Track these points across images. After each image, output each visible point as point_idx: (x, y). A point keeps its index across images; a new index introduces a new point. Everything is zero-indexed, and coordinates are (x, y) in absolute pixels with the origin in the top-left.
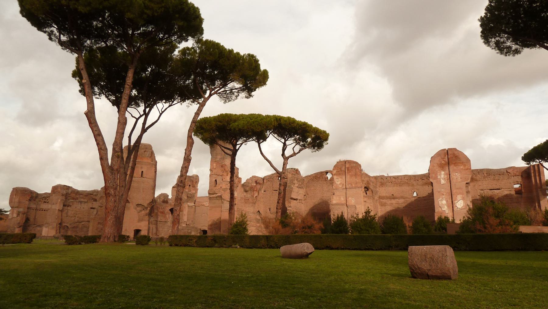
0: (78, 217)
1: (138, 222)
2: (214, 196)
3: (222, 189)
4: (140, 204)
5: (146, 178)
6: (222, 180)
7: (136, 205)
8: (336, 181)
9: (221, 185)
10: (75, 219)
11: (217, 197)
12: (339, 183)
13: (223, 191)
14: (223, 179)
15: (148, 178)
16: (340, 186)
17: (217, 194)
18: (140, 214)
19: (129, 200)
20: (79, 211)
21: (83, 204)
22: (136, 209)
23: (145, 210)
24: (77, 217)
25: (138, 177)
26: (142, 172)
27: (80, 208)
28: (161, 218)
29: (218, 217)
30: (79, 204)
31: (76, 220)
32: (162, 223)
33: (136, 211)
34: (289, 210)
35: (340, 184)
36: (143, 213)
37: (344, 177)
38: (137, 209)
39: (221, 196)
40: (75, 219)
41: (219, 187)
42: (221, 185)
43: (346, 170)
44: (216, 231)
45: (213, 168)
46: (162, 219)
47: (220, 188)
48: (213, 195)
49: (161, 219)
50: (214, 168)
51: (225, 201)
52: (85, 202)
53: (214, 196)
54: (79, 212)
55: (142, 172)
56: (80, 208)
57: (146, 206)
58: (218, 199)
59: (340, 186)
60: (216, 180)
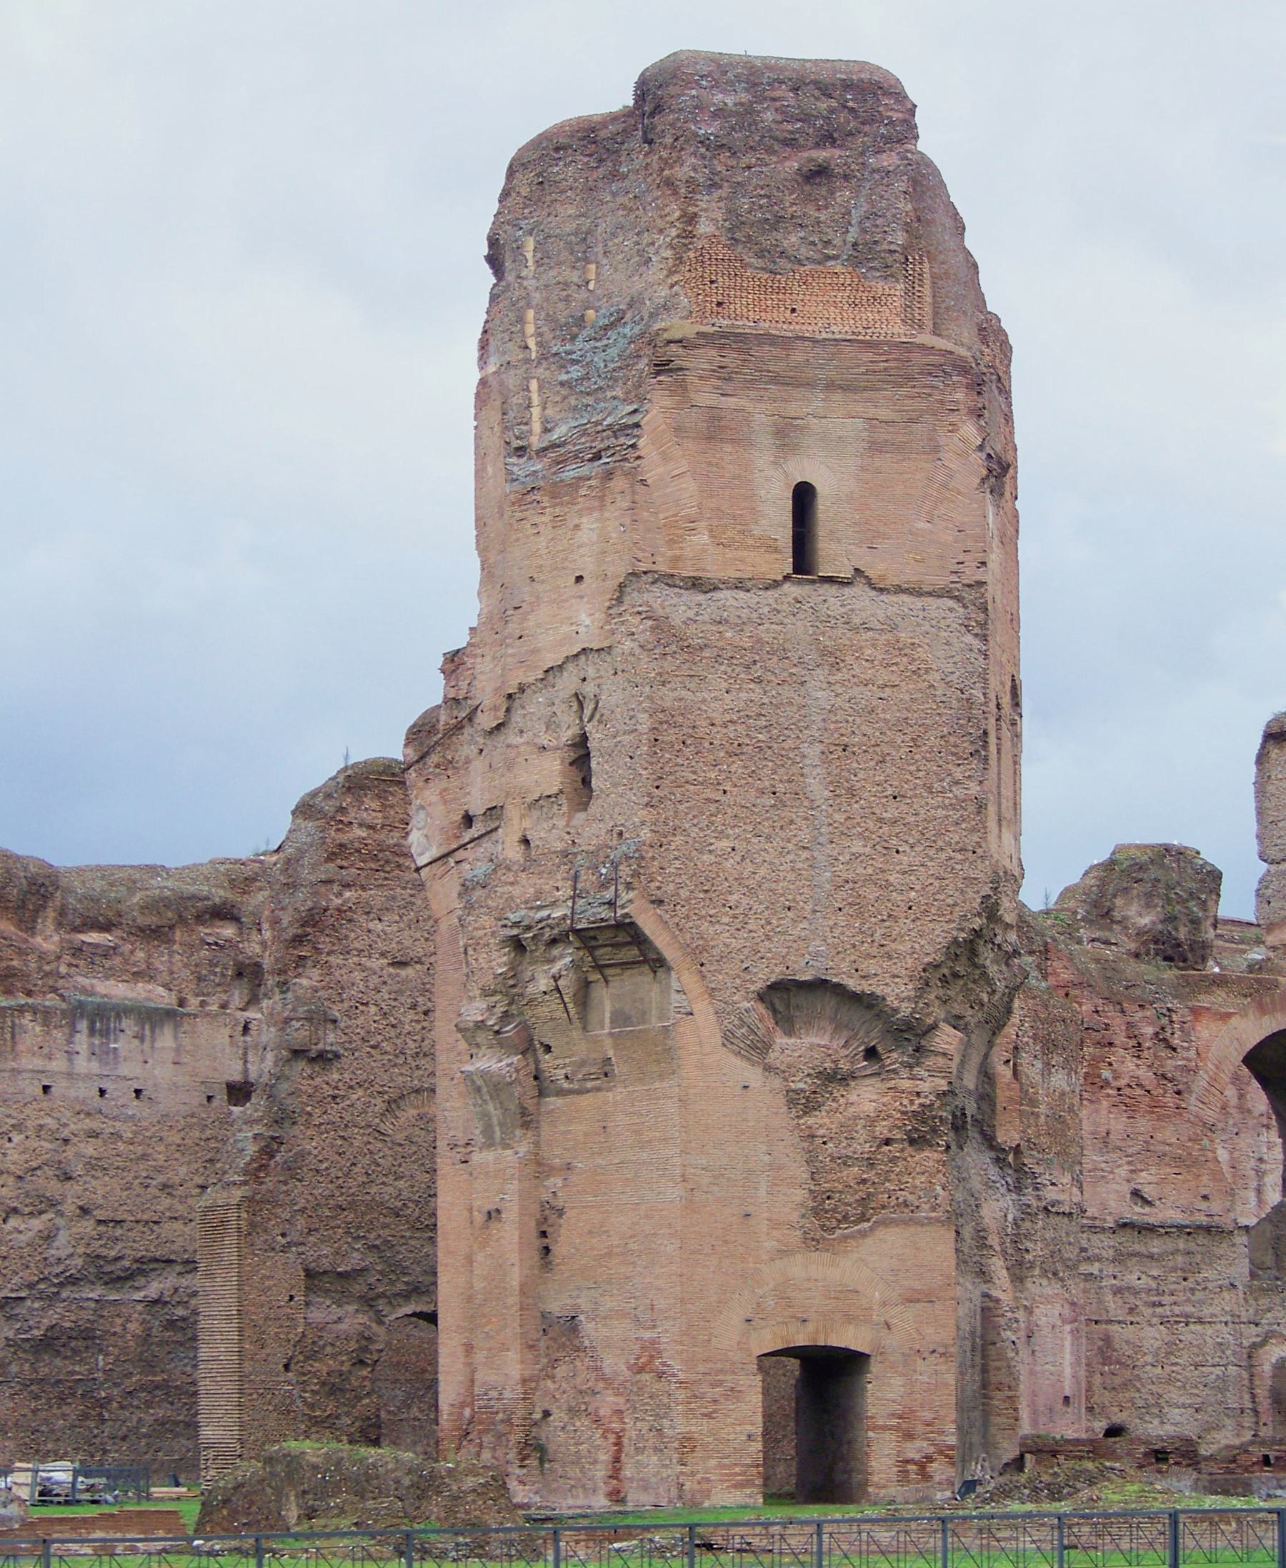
0: (84, 1211)
1: (813, 1242)
4: (820, 985)
5: (859, 591)
7: (761, 997)
10: (48, 1237)
15: (899, 590)
18: (820, 1121)
19: (647, 923)
20: (94, 1134)
21: (123, 1044)
22: (758, 1049)
23: (894, 1058)
24: (69, 1207)
25: (739, 585)
26: (803, 497)
27: (102, 1092)
28: (1146, 1180)
30: (82, 1041)
31: (62, 1245)
32: (1156, 1246)
33: (753, 1075)
36: (869, 1108)
38: (773, 1056)
40: (48, 1237)
46: (1148, 1191)
49: (1136, 1194)
52: (153, 1018)
54: (89, 1149)
55: (803, 497)
56: (102, 1092)
57: (905, 1009)
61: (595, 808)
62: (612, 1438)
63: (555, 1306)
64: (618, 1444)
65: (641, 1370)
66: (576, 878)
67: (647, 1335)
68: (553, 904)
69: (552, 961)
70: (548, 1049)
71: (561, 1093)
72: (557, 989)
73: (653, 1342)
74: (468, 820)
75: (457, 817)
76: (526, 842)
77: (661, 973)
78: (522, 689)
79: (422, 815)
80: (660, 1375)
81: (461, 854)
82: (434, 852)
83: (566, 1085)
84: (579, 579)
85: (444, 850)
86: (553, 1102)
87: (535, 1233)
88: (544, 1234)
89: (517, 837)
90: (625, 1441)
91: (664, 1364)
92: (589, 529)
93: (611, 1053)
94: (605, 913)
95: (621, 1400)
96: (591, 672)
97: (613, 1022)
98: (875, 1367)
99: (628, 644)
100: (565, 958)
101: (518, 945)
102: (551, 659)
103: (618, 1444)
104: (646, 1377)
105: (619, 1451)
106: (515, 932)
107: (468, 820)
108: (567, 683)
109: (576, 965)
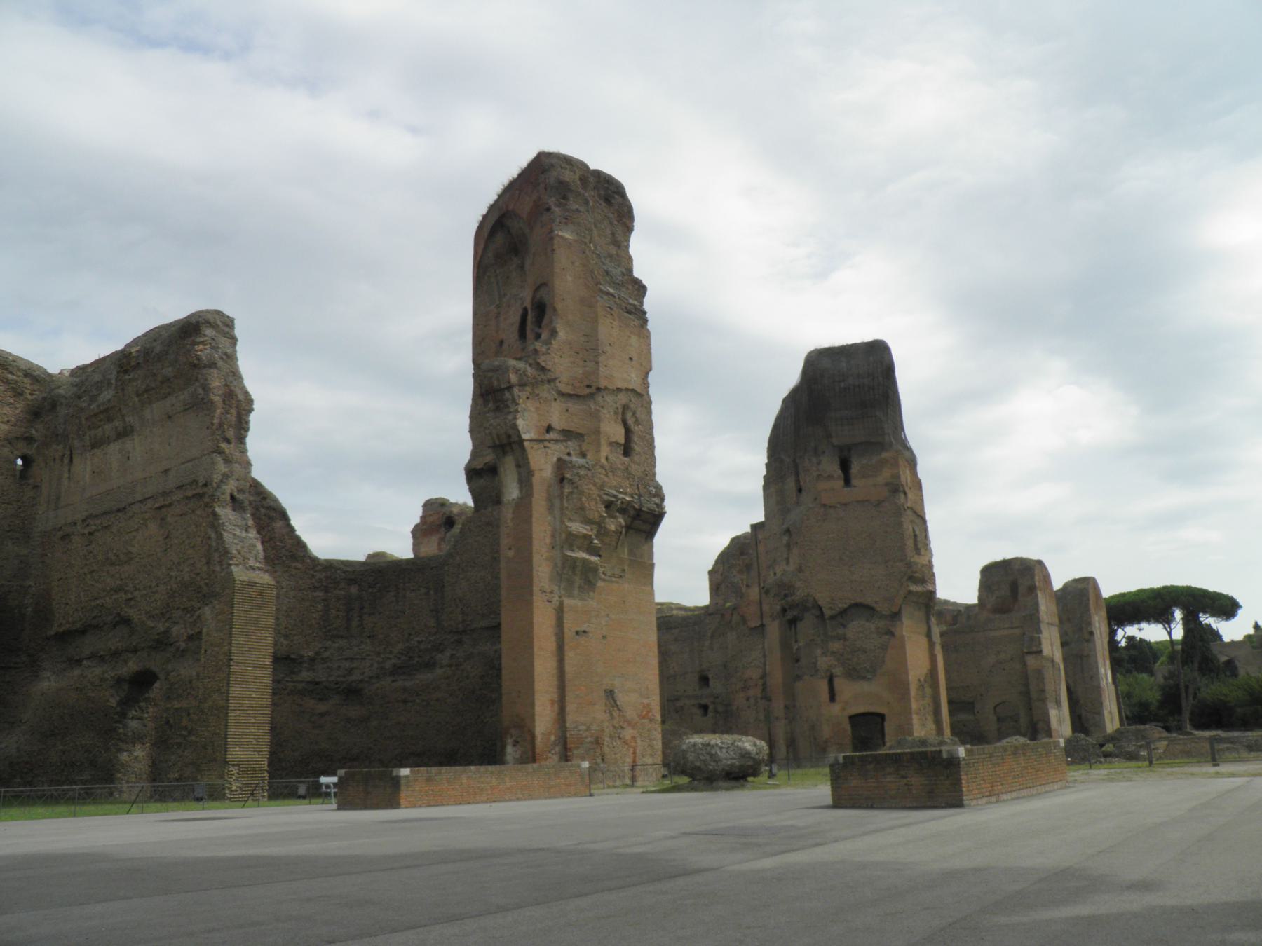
62: (631, 750)
64: (634, 753)
65: (643, 718)
67: (646, 701)
73: (648, 705)
74: (549, 429)
75: (546, 424)
78: (606, 388)
79: (526, 414)
81: (547, 444)
90: (638, 751)
91: (653, 715)
93: (626, 568)
95: (635, 732)
101: (608, 506)
103: (634, 753)
104: (646, 721)
105: (635, 757)
107: (549, 429)
108: (622, 399)
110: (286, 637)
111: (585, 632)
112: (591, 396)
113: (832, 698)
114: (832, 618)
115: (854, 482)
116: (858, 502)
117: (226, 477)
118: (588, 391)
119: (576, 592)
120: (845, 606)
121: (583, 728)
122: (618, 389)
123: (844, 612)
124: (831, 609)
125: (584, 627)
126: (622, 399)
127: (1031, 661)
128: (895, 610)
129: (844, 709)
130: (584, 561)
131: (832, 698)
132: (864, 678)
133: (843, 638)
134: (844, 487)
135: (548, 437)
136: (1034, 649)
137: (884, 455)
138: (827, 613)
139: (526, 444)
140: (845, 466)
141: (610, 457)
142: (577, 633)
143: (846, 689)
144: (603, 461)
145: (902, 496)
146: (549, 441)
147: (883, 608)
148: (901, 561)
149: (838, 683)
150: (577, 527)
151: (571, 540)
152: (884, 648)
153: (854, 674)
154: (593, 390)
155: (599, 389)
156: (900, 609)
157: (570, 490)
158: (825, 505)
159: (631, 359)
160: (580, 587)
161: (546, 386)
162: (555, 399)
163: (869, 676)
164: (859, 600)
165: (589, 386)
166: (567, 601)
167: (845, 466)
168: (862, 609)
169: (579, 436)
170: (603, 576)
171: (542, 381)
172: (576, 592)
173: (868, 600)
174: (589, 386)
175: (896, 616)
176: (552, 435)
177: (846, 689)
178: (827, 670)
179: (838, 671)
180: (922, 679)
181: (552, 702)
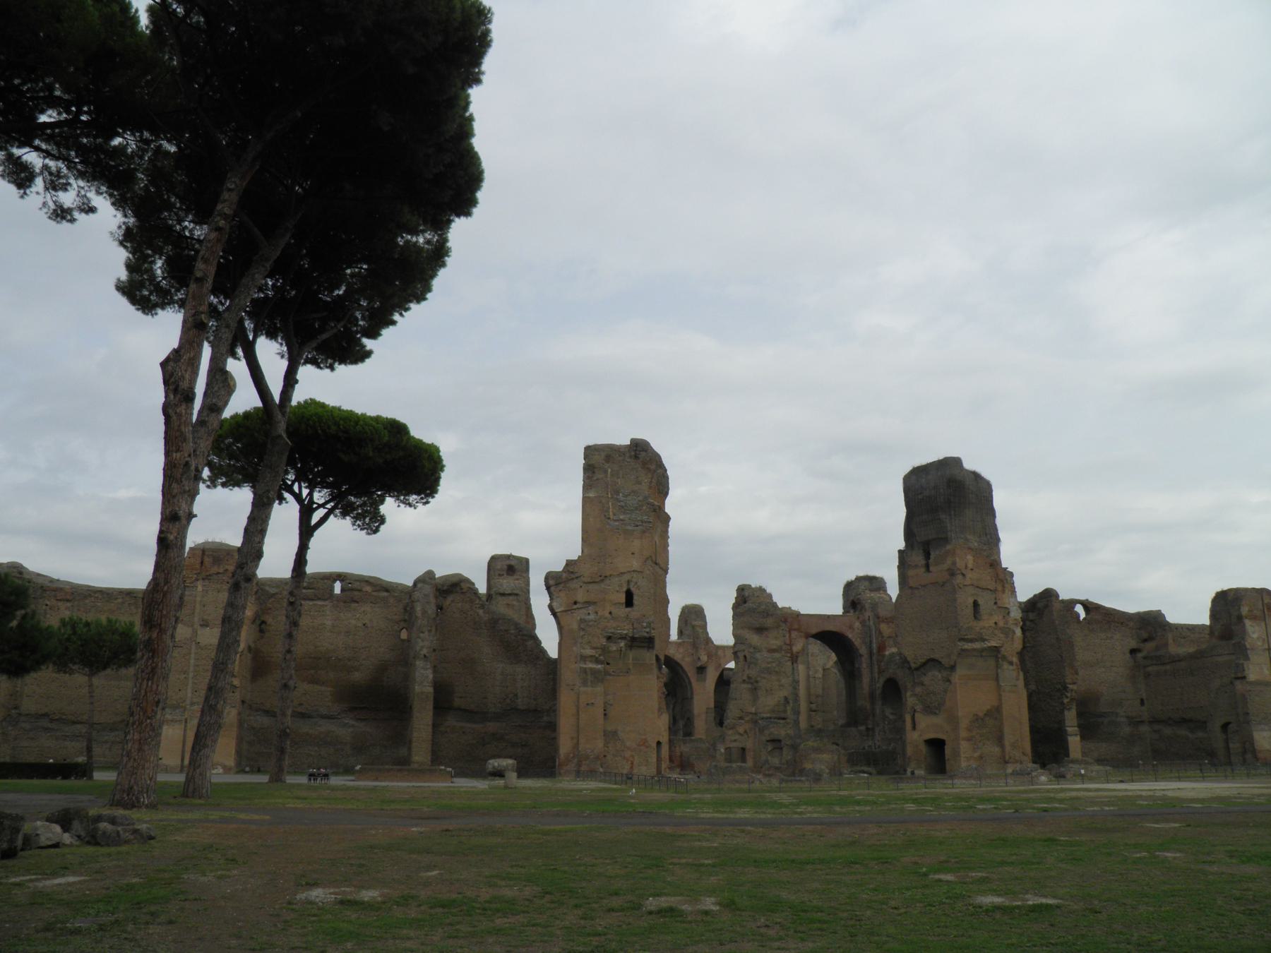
2: (977, 645)
3: (1000, 629)
6: (996, 603)
8: (1249, 631)
9: (995, 618)
11: (983, 650)
12: (1255, 636)
13: (1002, 635)
14: (998, 602)
16: (1260, 643)
17: (986, 640)
29: (989, 707)
34: (1072, 690)
35: (1258, 638)
37: (1263, 624)
39: (996, 650)
41: (991, 623)
42: (995, 618)
43: (1265, 610)
44: (984, 744)
45: (966, 567)
47: (994, 625)
48: (970, 644)
50: (970, 566)
51: (1005, 663)
53: (977, 645)
58: (981, 656)
59: (1260, 643)
60: (976, 604)
61: (635, 608)
62: (630, 762)
63: (609, 729)
64: (632, 763)
66: (633, 624)
67: (644, 737)
68: (624, 630)
69: (619, 643)
70: (608, 664)
71: (610, 675)
72: (621, 650)
74: (575, 603)
75: (573, 602)
76: (610, 613)
77: (651, 650)
78: (610, 575)
80: (647, 747)
81: (573, 611)
82: (562, 609)
83: (613, 674)
84: (633, 554)
85: (566, 609)
86: (608, 677)
87: (602, 710)
88: (605, 710)
89: (608, 612)
90: (635, 763)
92: (637, 543)
93: (631, 667)
94: (646, 634)
96: (635, 576)
97: (633, 660)
98: (663, 744)
99: (648, 572)
100: (622, 644)
101: (609, 638)
102: (622, 571)
104: (642, 747)
106: (611, 635)
109: (625, 645)
110: (535, 699)
111: (593, 703)
112: (602, 581)
113: (914, 728)
114: (917, 669)
115: (931, 568)
116: (932, 583)
117: (422, 647)
118: (600, 578)
119: (589, 683)
120: (923, 661)
121: (590, 751)
122: (622, 573)
123: (924, 664)
124: (915, 663)
125: (593, 701)
126: (626, 577)
127: (1239, 686)
128: (952, 663)
129: (921, 735)
130: (591, 669)
131: (914, 728)
132: (935, 713)
133: (922, 684)
134: (924, 572)
135: (575, 607)
136: (1240, 675)
137: (948, 547)
138: (913, 666)
139: (558, 614)
140: (927, 555)
141: (613, 611)
142: (588, 704)
143: (924, 721)
144: (607, 615)
145: (960, 577)
146: (575, 609)
147: (944, 661)
148: (956, 627)
149: (916, 715)
150: (589, 652)
151: (584, 658)
152: (946, 691)
153: (930, 710)
154: (602, 578)
155: (606, 577)
156: (955, 663)
157: (583, 633)
158: (911, 588)
159: (633, 554)
160: (591, 681)
161: (575, 581)
162: (581, 587)
163: (937, 712)
164: (932, 657)
165: (601, 576)
166: (582, 689)
167: (927, 555)
168: (932, 662)
169: (595, 603)
170: (613, 674)
171: (573, 579)
172: (589, 683)
173: (936, 656)
174: (601, 576)
175: (953, 668)
176: (578, 606)
177: (924, 721)
178: (913, 707)
179: (918, 708)
180: (981, 714)
181: (572, 738)
